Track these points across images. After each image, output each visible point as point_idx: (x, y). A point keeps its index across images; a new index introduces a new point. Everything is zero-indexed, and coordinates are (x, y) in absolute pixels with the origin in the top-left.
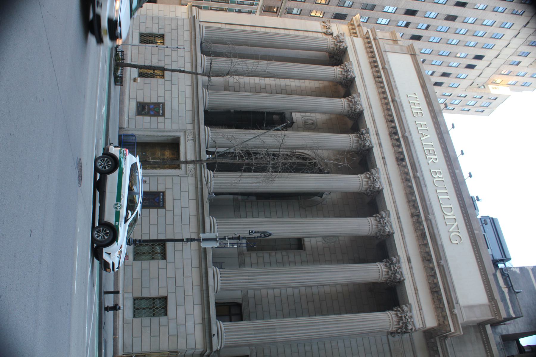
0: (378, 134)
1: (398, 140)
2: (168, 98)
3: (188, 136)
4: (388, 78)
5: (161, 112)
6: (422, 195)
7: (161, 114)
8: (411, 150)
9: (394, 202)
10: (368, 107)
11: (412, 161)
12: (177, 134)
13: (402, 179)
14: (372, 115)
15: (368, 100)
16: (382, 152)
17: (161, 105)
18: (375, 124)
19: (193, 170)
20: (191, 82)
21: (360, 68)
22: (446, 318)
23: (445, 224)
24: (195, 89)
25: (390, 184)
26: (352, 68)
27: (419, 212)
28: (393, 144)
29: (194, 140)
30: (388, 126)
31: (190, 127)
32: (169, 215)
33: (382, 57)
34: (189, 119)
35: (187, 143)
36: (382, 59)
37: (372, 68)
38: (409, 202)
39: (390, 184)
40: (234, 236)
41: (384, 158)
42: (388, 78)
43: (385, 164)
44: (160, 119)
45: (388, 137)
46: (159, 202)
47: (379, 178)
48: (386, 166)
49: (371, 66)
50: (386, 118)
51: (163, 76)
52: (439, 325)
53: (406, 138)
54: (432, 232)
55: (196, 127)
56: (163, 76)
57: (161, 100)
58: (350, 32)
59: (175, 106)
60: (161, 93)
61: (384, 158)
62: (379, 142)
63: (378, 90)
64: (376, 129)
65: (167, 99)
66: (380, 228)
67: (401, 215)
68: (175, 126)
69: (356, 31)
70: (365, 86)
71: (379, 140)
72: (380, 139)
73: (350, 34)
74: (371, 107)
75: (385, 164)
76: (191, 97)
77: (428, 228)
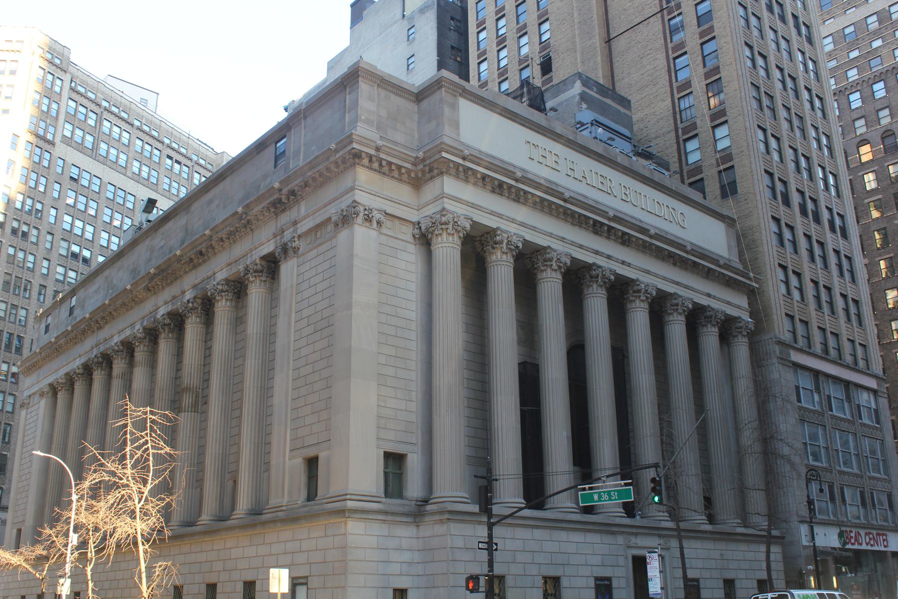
0: (597, 251)
1: (610, 228)
2: (586, 571)
3: (632, 542)
4: (534, 184)
5: (606, 582)
6: (669, 241)
7: (608, 583)
8: (627, 221)
9: (664, 279)
10: (561, 243)
11: (637, 228)
12: (630, 558)
13: (642, 251)
14: (573, 244)
15: (553, 236)
16: (616, 260)
17: (598, 582)
18: (584, 248)
19: (665, 539)
20: (563, 531)
21: (504, 217)
22: (672, 255)
23: (574, 180)
24: (572, 526)
25: (648, 272)
26: (512, 234)
27: (679, 255)
28: (605, 237)
29: (636, 535)
30: (585, 228)
31: (620, 539)
32: (706, 574)
33: (500, 169)
34: (608, 539)
35: (639, 545)
36: (503, 171)
37: (502, 195)
38: (663, 259)
39: (648, 272)
40: (807, 507)
41: (623, 263)
42: (534, 184)
43: (629, 265)
44: (615, 584)
45: (597, 238)
46: (694, 585)
47: (648, 285)
48: (631, 266)
49: (498, 194)
50: (576, 225)
51: (502, 578)
52: (747, 294)
53: (616, 219)
54: (698, 254)
55: (623, 529)
56: (502, 578)
57: (592, 582)
58: (375, 170)
59: (596, 560)
60: (581, 582)
61: (623, 263)
62: (606, 256)
63: (537, 209)
64: (592, 251)
65: (589, 574)
66: (746, 334)
67: (677, 280)
68: (621, 560)
69: (386, 160)
70: (532, 228)
71: (604, 255)
72: (603, 253)
73: (380, 172)
74: (564, 238)
75: (629, 265)
76: (583, 533)
77: (693, 256)
